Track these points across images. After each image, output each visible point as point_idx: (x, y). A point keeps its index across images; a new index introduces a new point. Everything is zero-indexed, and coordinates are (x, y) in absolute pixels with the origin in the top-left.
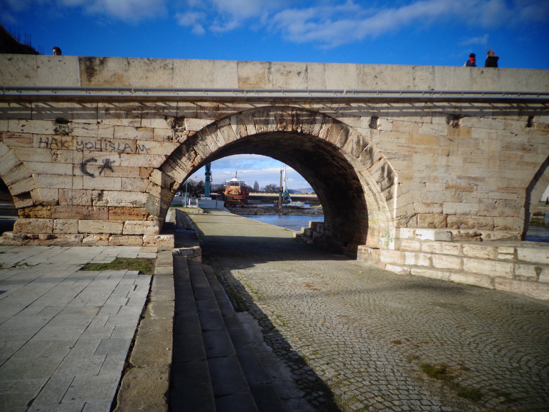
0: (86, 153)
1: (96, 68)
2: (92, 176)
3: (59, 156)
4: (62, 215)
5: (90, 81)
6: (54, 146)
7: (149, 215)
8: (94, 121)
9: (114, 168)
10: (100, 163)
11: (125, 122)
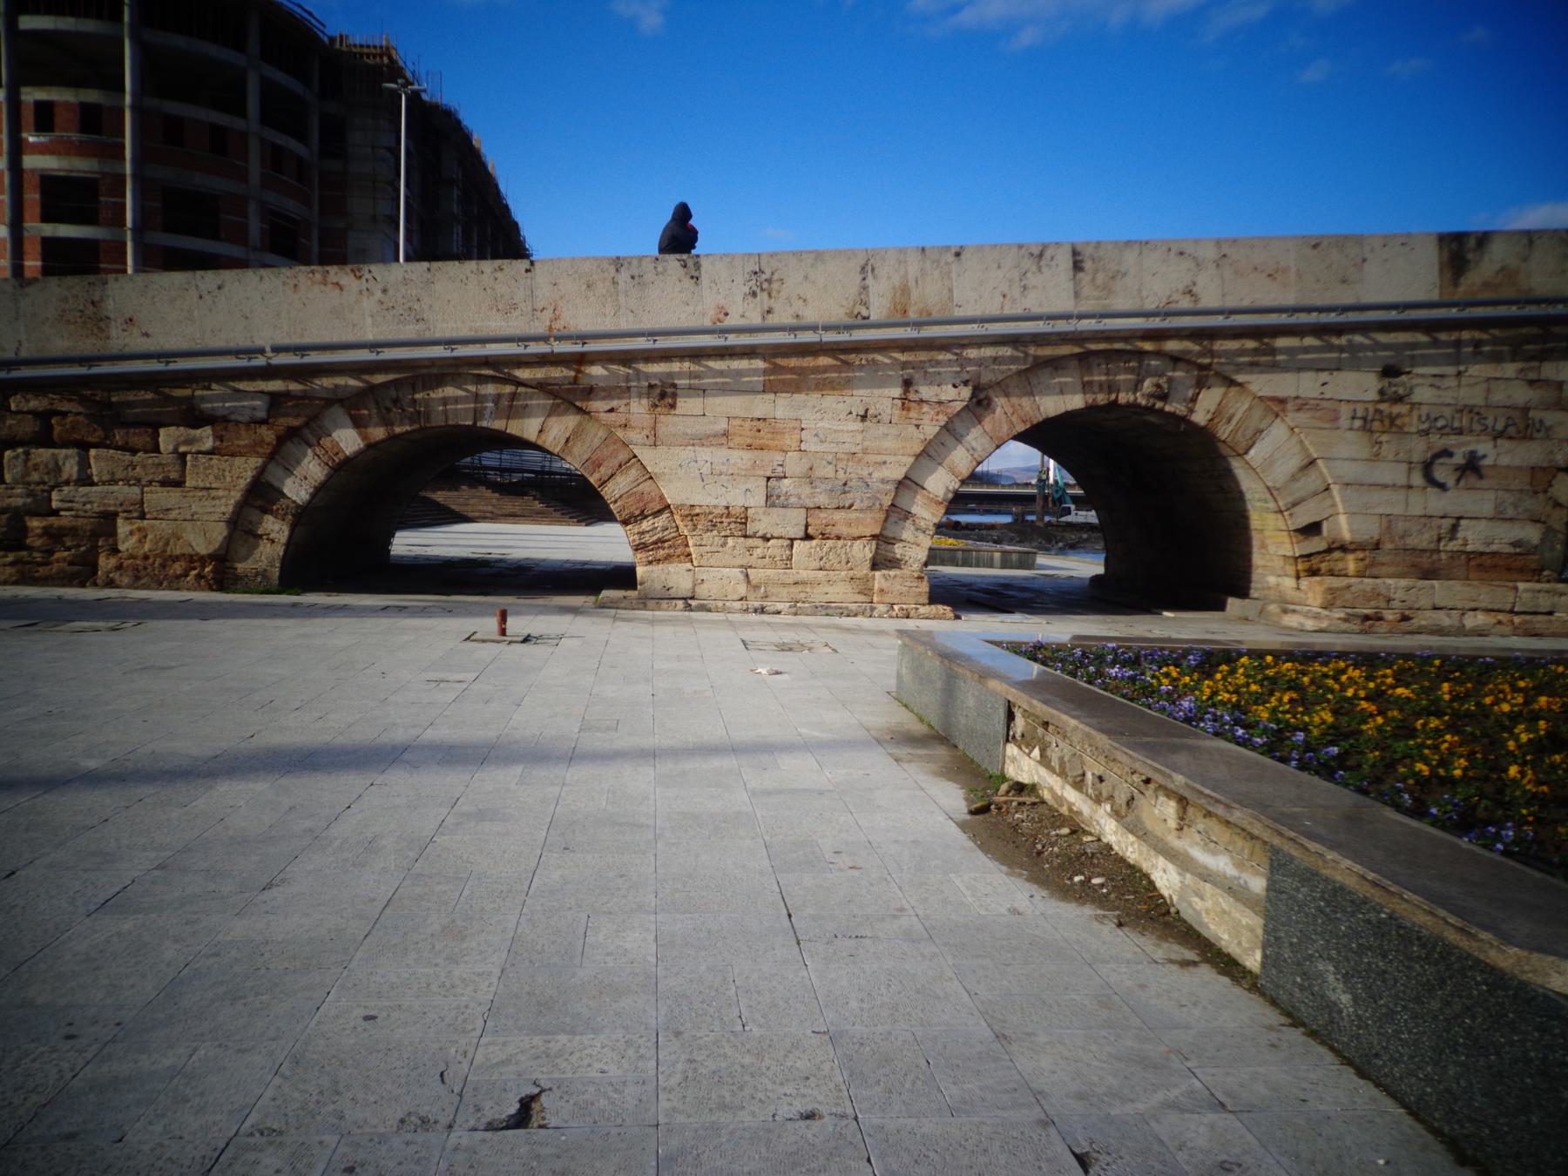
0: (1434, 438)
1: (1470, 256)
2: (1442, 487)
3: (1385, 447)
4: (1384, 570)
5: (1455, 282)
6: (1376, 425)
7: (1543, 569)
8: (1450, 370)
9: (1484, 471)
10: (1459, 459)
11: (1510, 369)
